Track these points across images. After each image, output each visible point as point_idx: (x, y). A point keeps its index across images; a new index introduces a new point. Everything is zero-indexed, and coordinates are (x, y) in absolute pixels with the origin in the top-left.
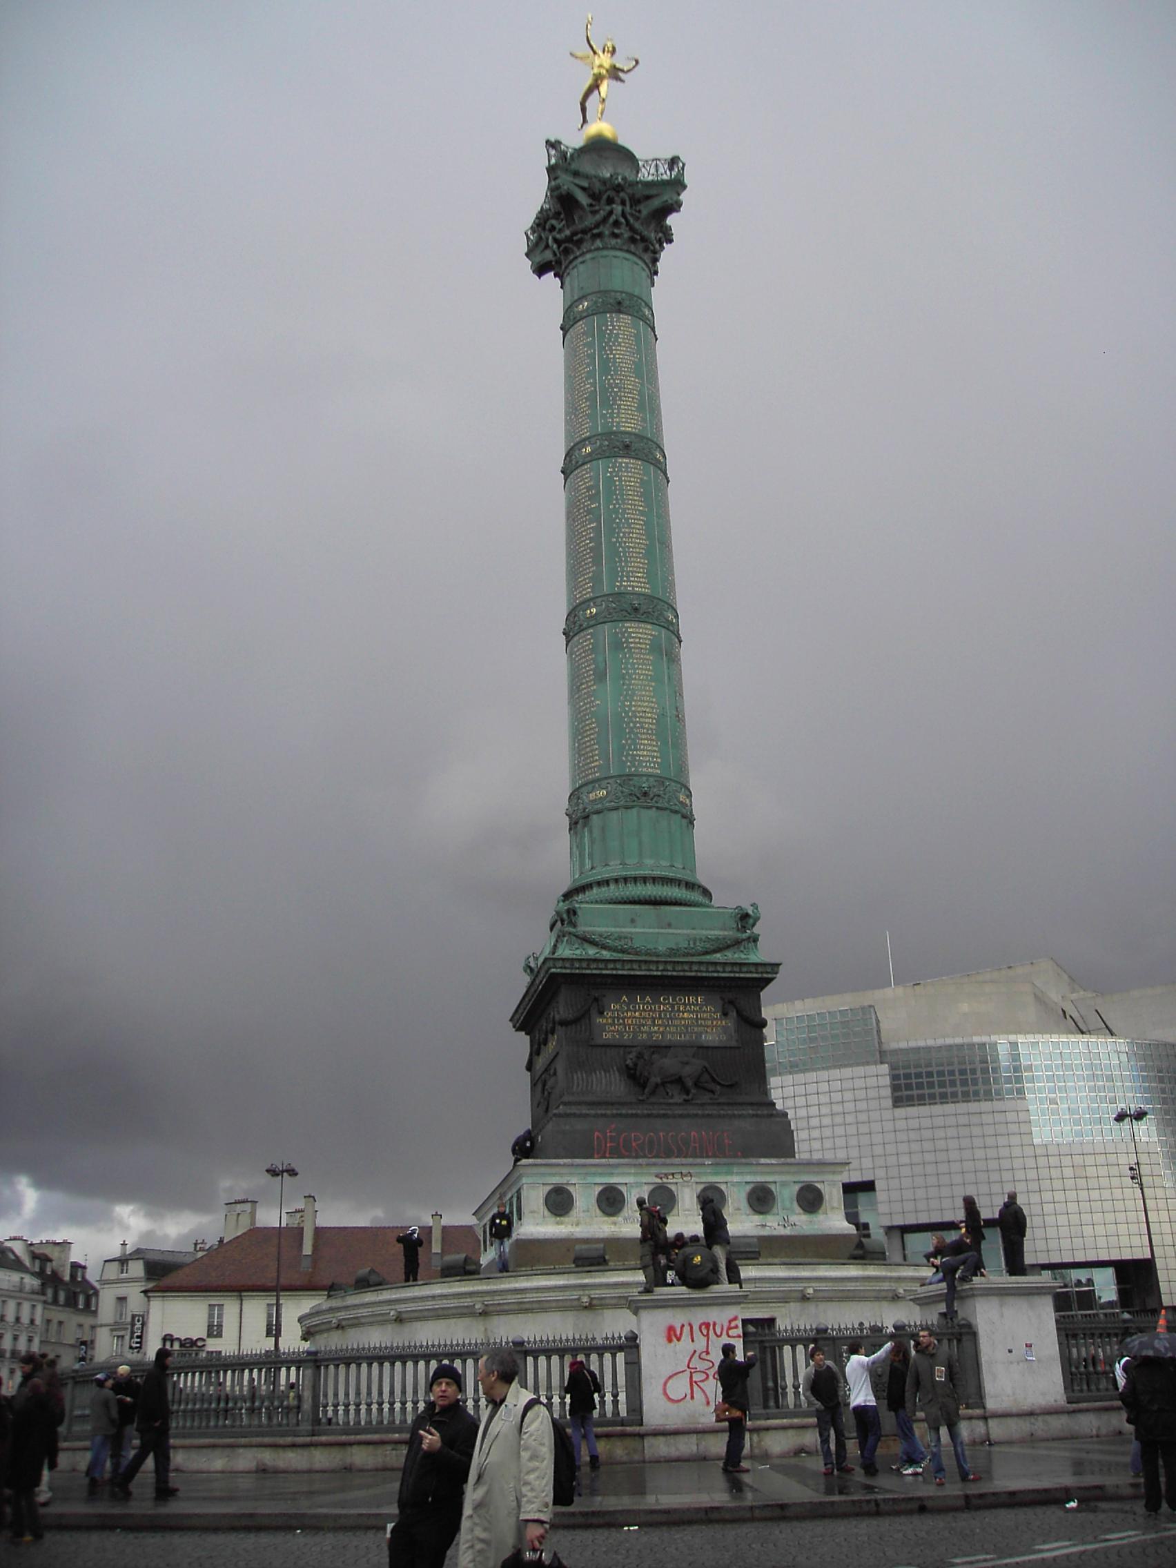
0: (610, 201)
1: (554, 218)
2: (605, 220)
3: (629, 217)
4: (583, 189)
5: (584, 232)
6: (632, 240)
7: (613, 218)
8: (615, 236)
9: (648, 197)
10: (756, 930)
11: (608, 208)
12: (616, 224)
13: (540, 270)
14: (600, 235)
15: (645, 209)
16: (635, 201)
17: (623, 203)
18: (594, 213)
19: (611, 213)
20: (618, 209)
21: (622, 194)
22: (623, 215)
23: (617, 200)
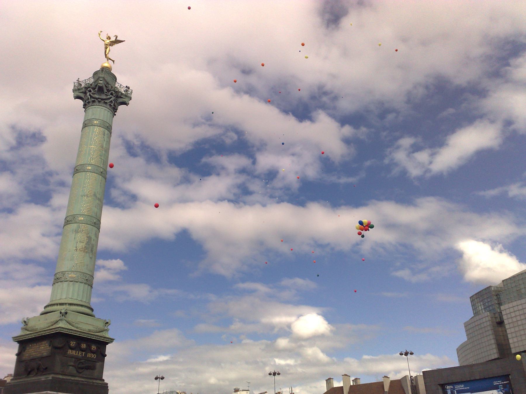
0: (112, 94)
1: (92, 88)
5: (102, 99)
8: (110, 105)
9: (121, 97)
11: (111, 96)
12: (111, 102)
13: (77, 97)
14: (106, 103)
16: (117, 97)
18: (107, 95)
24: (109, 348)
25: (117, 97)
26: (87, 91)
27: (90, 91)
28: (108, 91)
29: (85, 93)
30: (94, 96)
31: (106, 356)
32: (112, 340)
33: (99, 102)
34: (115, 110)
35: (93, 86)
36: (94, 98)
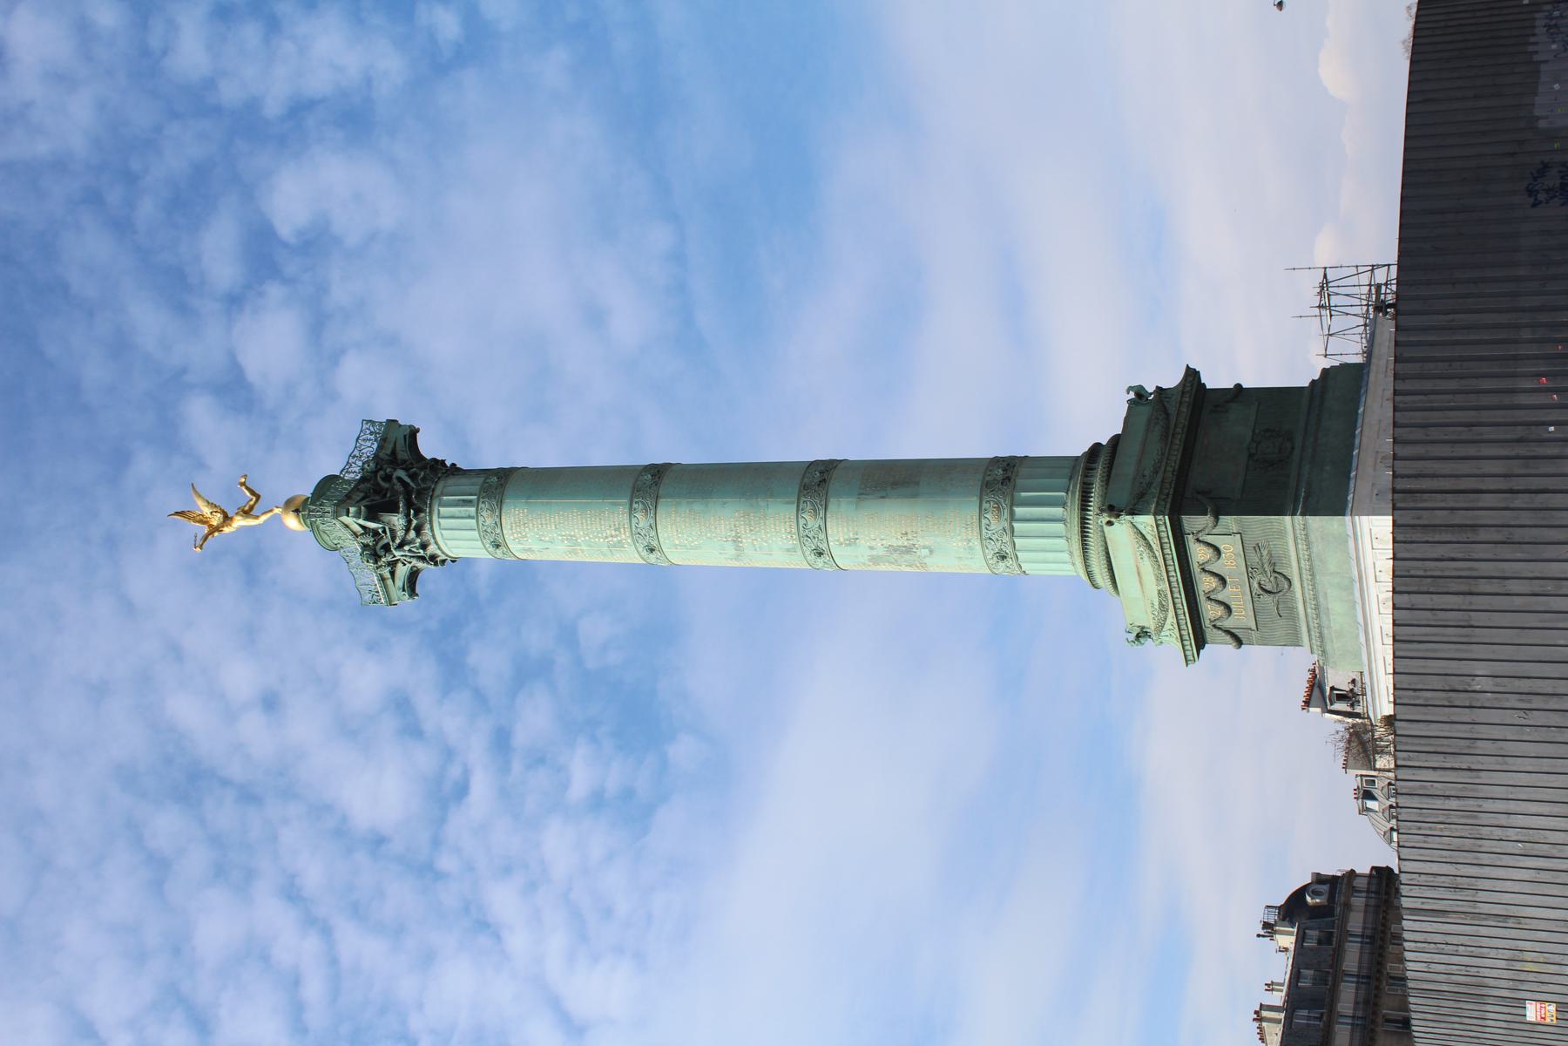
0: (388, 478)
7: (408, 480)
9: (394, 453)
10: (1150, 389)
12: (413, 477)
14: (421, 493)
19: (400, 479)
20: (401, 473)
24: (1214, 379)
25: (394, 460)
26: (390, 558)
27: (387, 548)
29: (393, 564)
30: (400, 534)
31: (1238, 386)
32: (1192, 375)
33: (418, 512)
34: (437, 465)
35: (369, 540)
36: (407, 530)
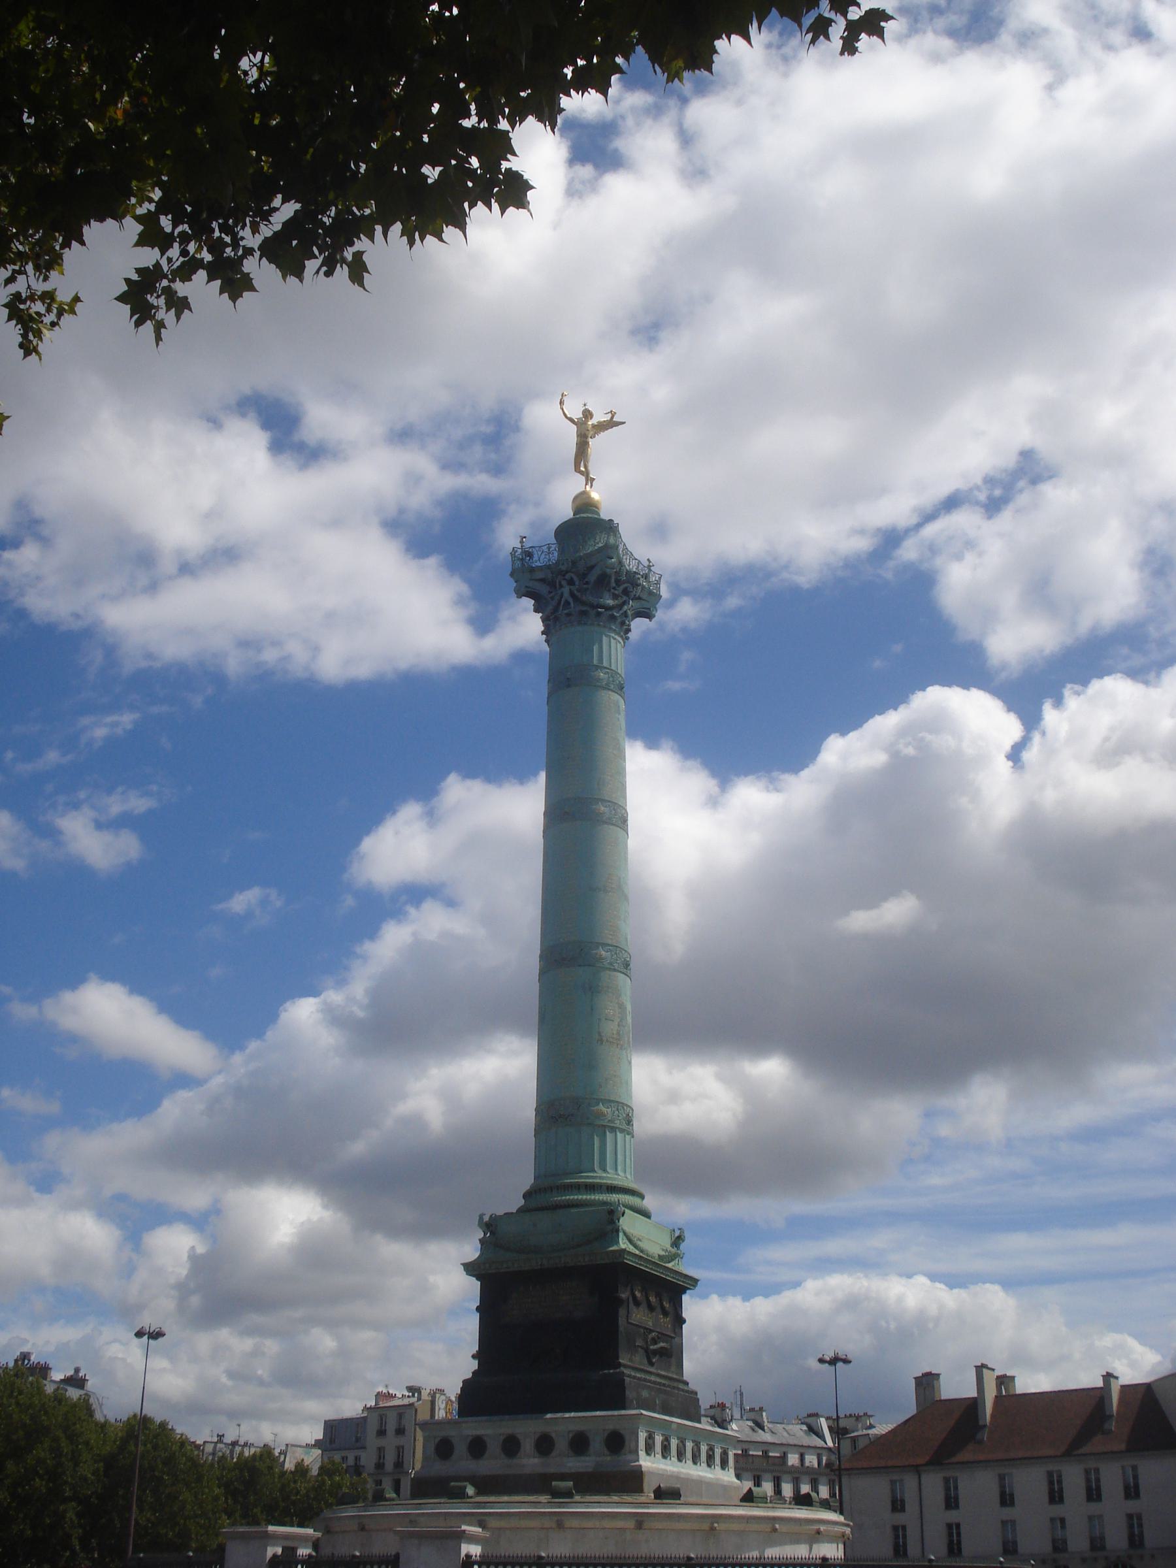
2: (559, 603)
3: (578, 594)
4: (542, 580)
6: (584, 613)
15: (592, 577)
17: (571, 582)
18: (552, 598)
20: (566, 590)
21: (568, 576)
22: (572, 594)
23: (564, 583)
28: (552, 584)
